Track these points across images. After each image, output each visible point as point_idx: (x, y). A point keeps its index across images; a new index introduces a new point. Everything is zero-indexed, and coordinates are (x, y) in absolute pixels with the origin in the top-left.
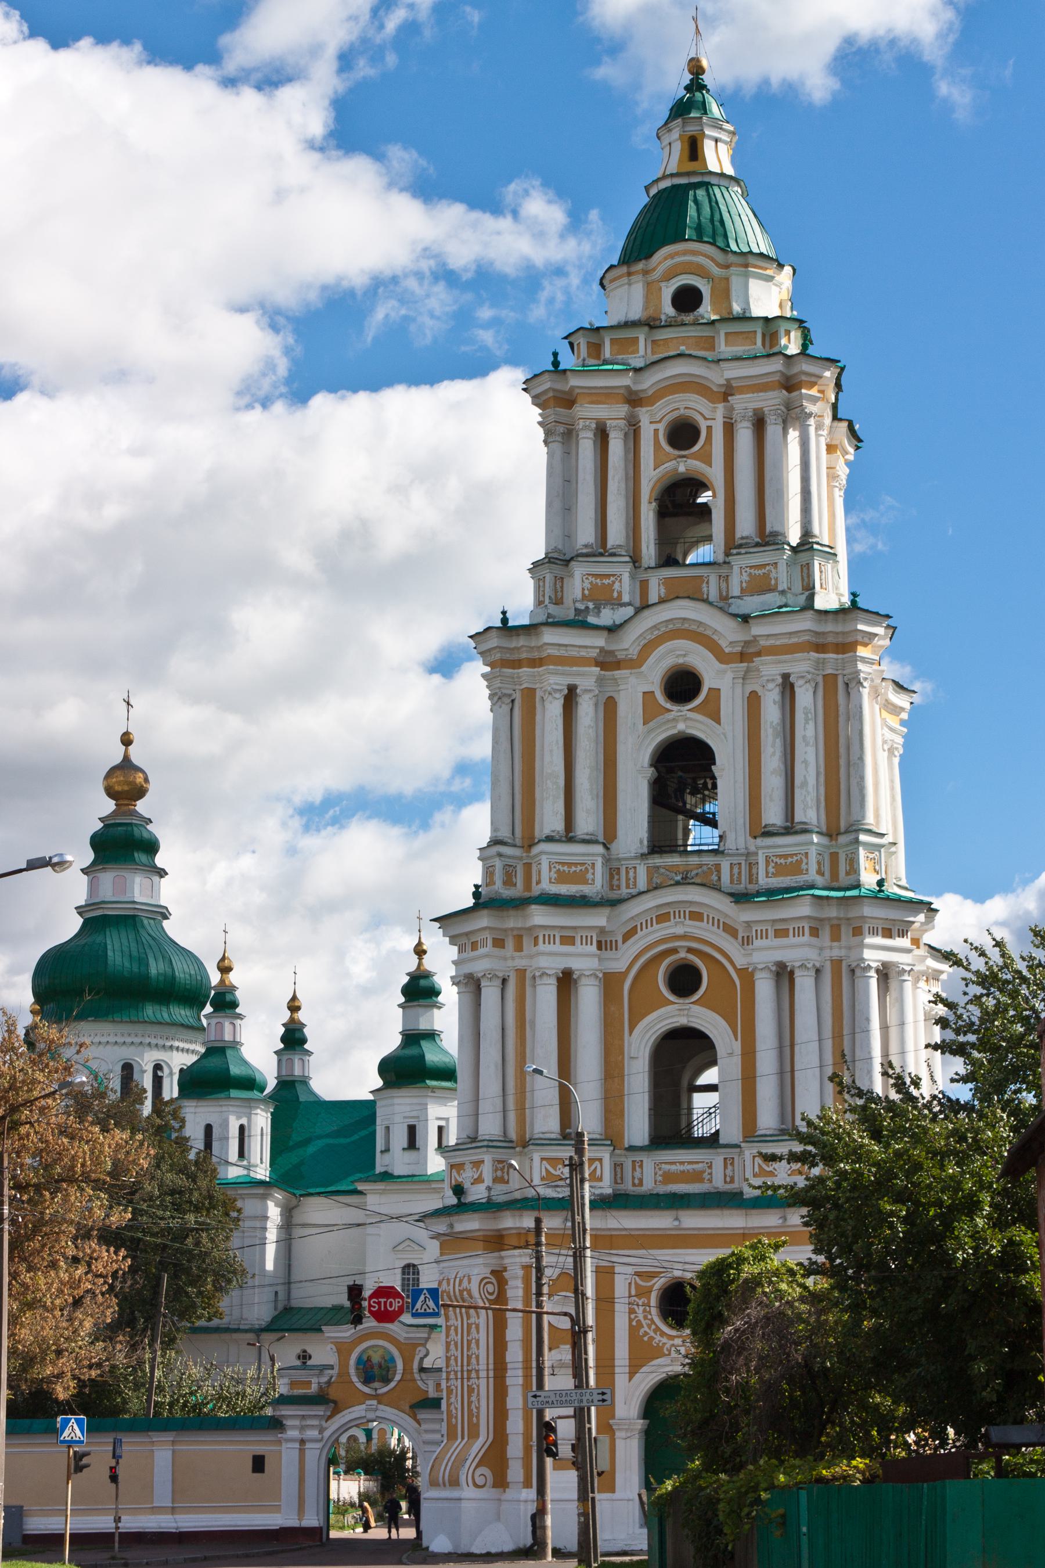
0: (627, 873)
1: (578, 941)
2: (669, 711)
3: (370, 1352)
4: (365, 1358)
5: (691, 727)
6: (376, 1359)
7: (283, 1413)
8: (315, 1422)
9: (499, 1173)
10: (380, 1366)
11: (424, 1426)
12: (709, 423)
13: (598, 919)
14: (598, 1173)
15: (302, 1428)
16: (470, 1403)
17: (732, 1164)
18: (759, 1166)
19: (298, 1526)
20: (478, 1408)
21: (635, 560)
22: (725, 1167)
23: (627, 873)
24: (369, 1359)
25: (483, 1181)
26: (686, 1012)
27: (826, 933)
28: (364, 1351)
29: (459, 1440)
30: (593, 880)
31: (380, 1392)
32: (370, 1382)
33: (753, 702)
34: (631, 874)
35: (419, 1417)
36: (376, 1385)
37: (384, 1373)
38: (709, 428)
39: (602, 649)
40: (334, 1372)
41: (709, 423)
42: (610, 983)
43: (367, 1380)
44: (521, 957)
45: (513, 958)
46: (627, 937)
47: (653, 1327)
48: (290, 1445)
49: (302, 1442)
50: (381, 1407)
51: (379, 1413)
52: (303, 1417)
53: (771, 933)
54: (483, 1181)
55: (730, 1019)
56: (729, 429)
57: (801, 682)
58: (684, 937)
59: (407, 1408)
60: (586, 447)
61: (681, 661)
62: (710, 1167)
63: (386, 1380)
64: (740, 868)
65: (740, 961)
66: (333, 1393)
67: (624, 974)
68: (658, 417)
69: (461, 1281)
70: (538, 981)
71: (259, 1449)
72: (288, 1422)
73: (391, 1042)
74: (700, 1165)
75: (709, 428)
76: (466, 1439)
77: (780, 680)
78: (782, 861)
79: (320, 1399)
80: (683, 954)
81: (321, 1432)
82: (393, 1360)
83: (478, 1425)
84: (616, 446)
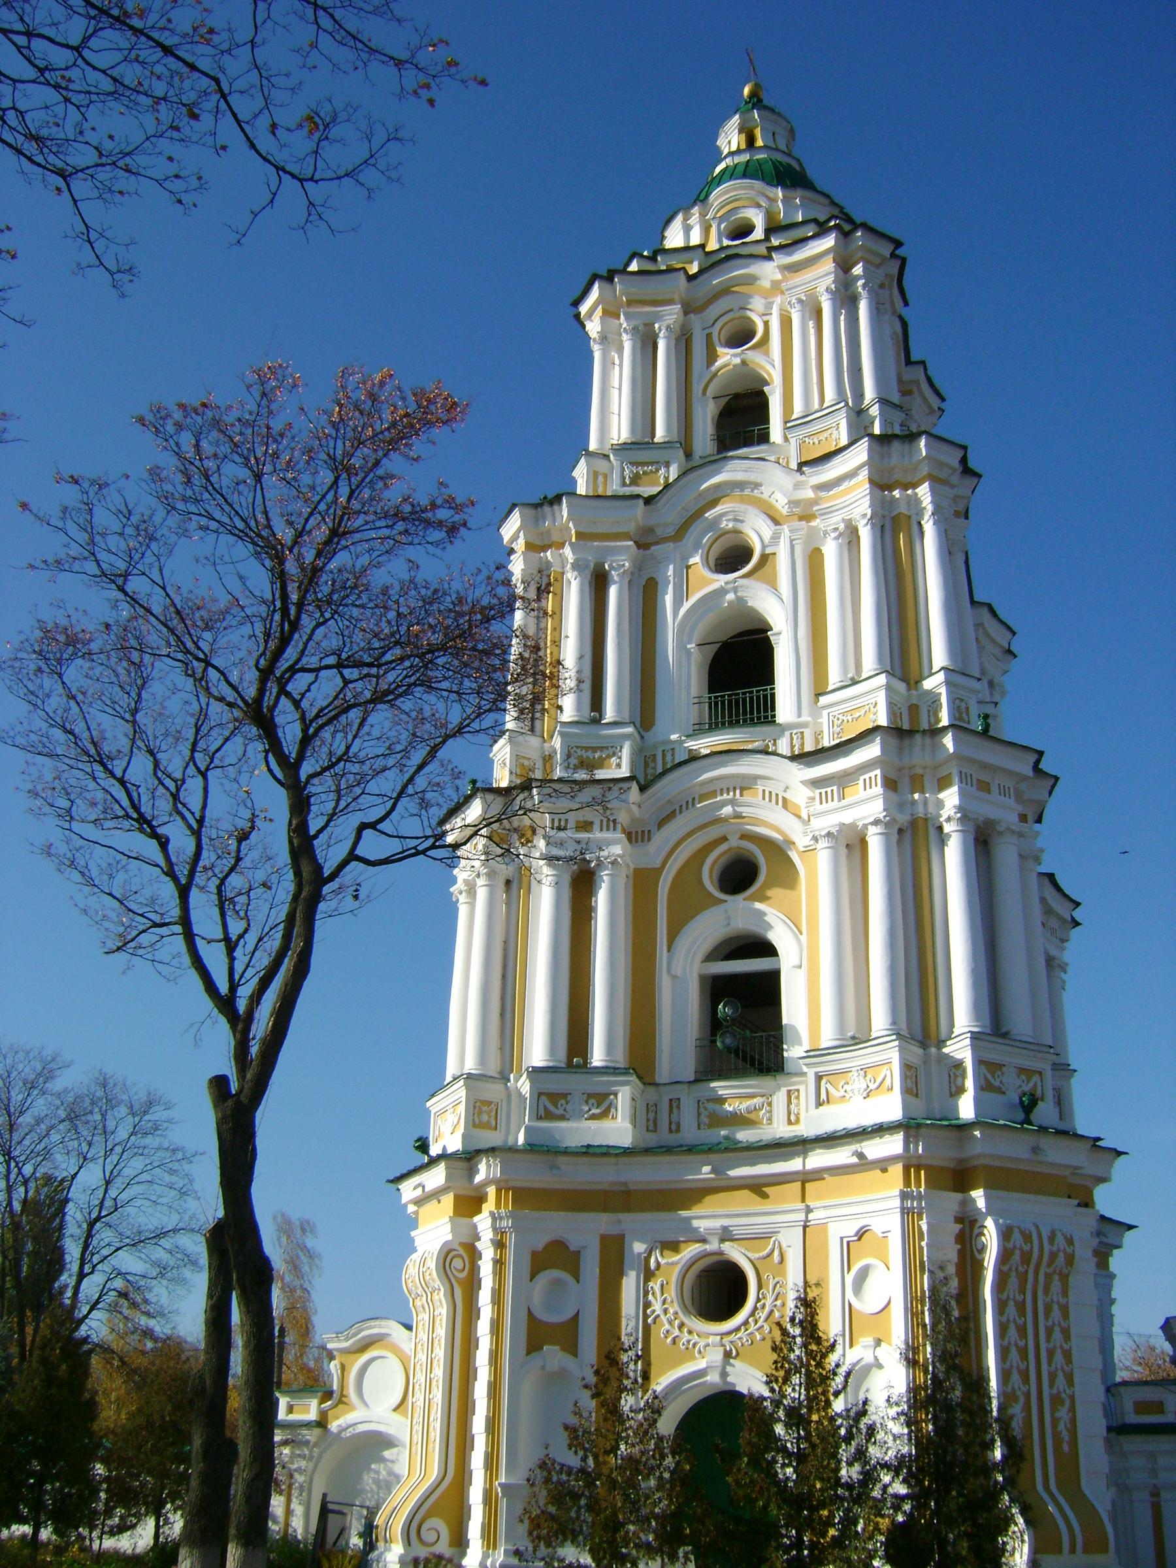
0: (664, 756)
1: (597, 826)
9: (485, 1118)
12: (766, 318)
17: (798, 1098)
21: (688, 455)
23: (664, 756)
27: (905, 784)
30: (619, 766)
33: (815, 560)
34: (669, 758)
38: (766, 324)
41: (766, 318)
42: (642, 884)
46: (661, 824)
47: (677, 1322)
64: (802, 738)
75: (766, 324)
77: (842, 526)
80: (734, 842)
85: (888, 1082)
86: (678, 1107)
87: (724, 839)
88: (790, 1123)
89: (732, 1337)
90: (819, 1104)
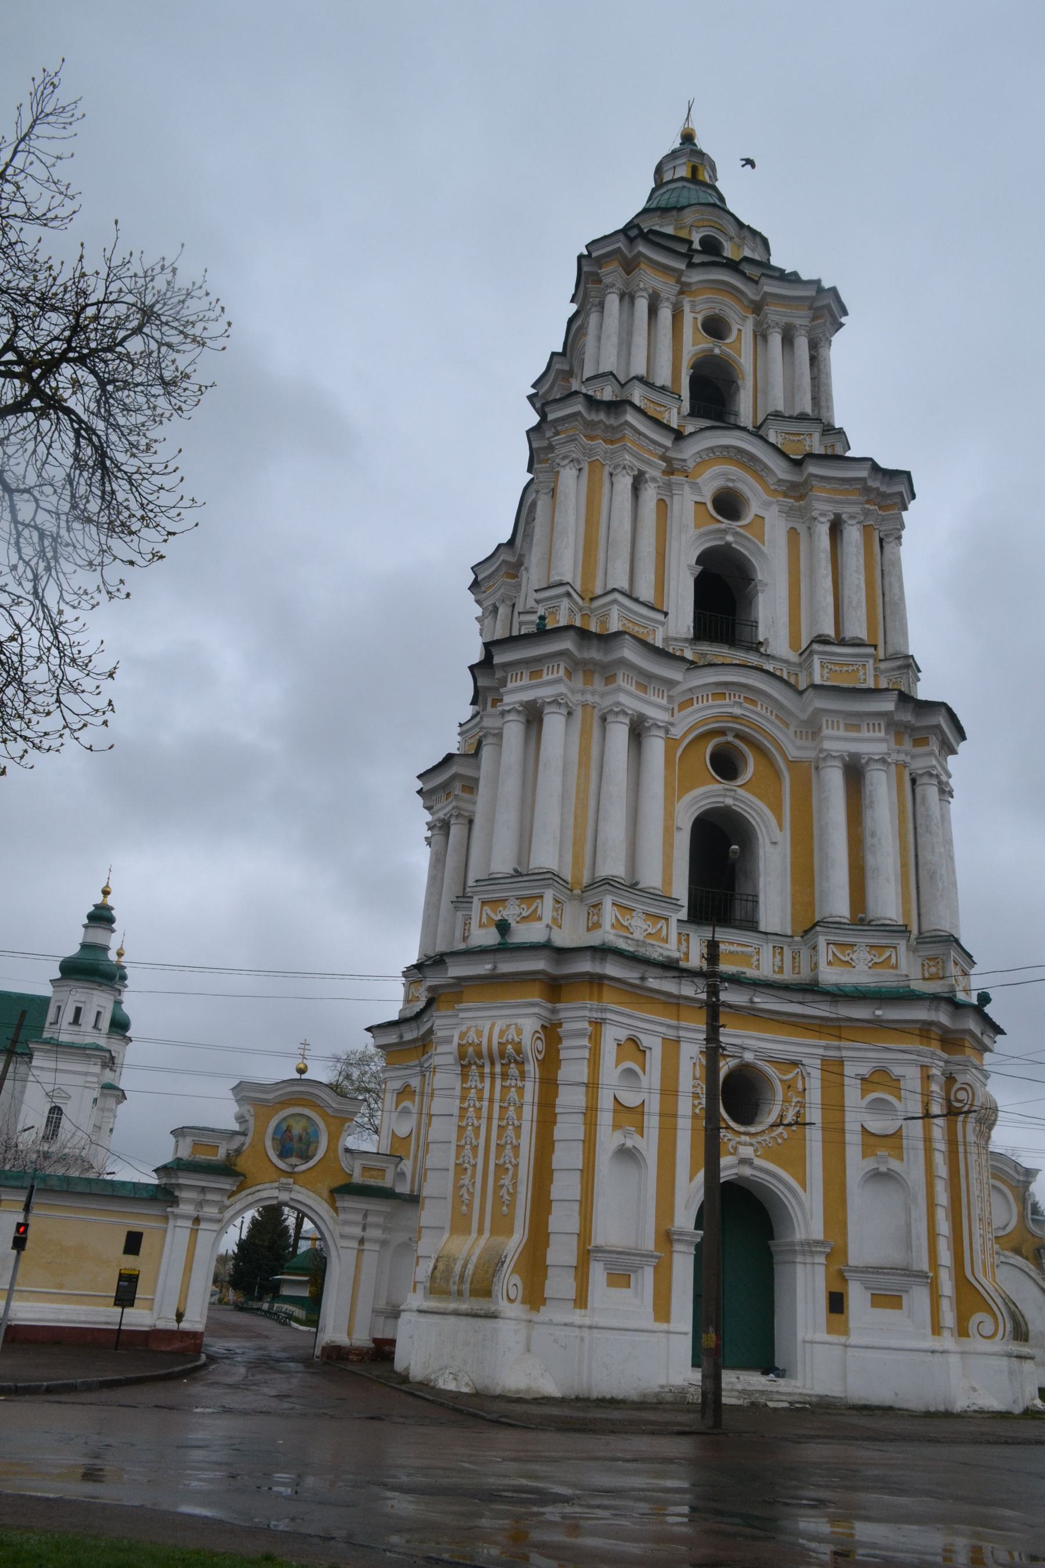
2: (719, 521)
3: (291, 1122)
4: (284, 1127)
5: (736, 542)
6: (297, 1129)
7: (181, 1181)
8: (216, 1197)
10: (300, 1139)
11: (342, 1216)
12: (740, 327)
13: (675, 673)
14: (664, 933)
15: (200, 1204)
16: (498, 1187)
18: (834, 954)
19: (175, 1328)
20: (513, 1195)
22: (774, 956)
24: (289, 1130)
25: (540, 919)
26: (732, 794)
28: (285, 1119)
29: (474, 1235)
31: (297, 1169)
32: (286, 1157)
35: (339, 1204)
36: (294, 1160)
37: (304, 1147)
39: (667, 448)
40: (248, 1140)
43: (283, 1155)
44: (593, 693)
45: (583, 693)
46: (682, 706)
48: (180, 1223)
49: (197, 1220)
50: (297, 1187)
51: (294, 1196)
52: (203, 1190)
53: (842, 726)
54: (540, 919)
55: (777, 809)
56: (761, 336)
57: (851, 522)
58: (735, 718)
59: (326, 1193)
60: (642, 305)
61: (731, 485)
62: (758, 953)
63: (306, 1157)
65: (793, 753)
66: (242, 1164)
67: (678, 742)
68: (698, 309)
69: (502, 1033)
70: (610, 718)
71: (136, 1224)
72: (183, 1194)
73: (72, 949)
74: (749, 949)
76: (487, 1234)
78: (837, 668)
79: (226, 1169)
80: (730, 738)
81: (221, 1212)
82: (316, 1133)
83: (510, 1217)
84: (665, 314)
85: (893, 960)
86: (688, 941)
87: (722, 732)
88: (774, 971)
89: (760, 1138)
90: (829, 963)
